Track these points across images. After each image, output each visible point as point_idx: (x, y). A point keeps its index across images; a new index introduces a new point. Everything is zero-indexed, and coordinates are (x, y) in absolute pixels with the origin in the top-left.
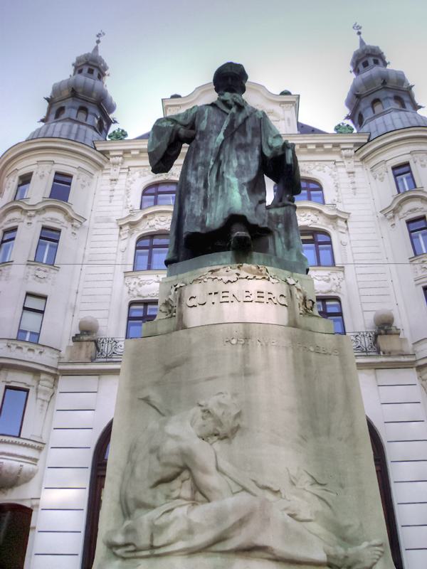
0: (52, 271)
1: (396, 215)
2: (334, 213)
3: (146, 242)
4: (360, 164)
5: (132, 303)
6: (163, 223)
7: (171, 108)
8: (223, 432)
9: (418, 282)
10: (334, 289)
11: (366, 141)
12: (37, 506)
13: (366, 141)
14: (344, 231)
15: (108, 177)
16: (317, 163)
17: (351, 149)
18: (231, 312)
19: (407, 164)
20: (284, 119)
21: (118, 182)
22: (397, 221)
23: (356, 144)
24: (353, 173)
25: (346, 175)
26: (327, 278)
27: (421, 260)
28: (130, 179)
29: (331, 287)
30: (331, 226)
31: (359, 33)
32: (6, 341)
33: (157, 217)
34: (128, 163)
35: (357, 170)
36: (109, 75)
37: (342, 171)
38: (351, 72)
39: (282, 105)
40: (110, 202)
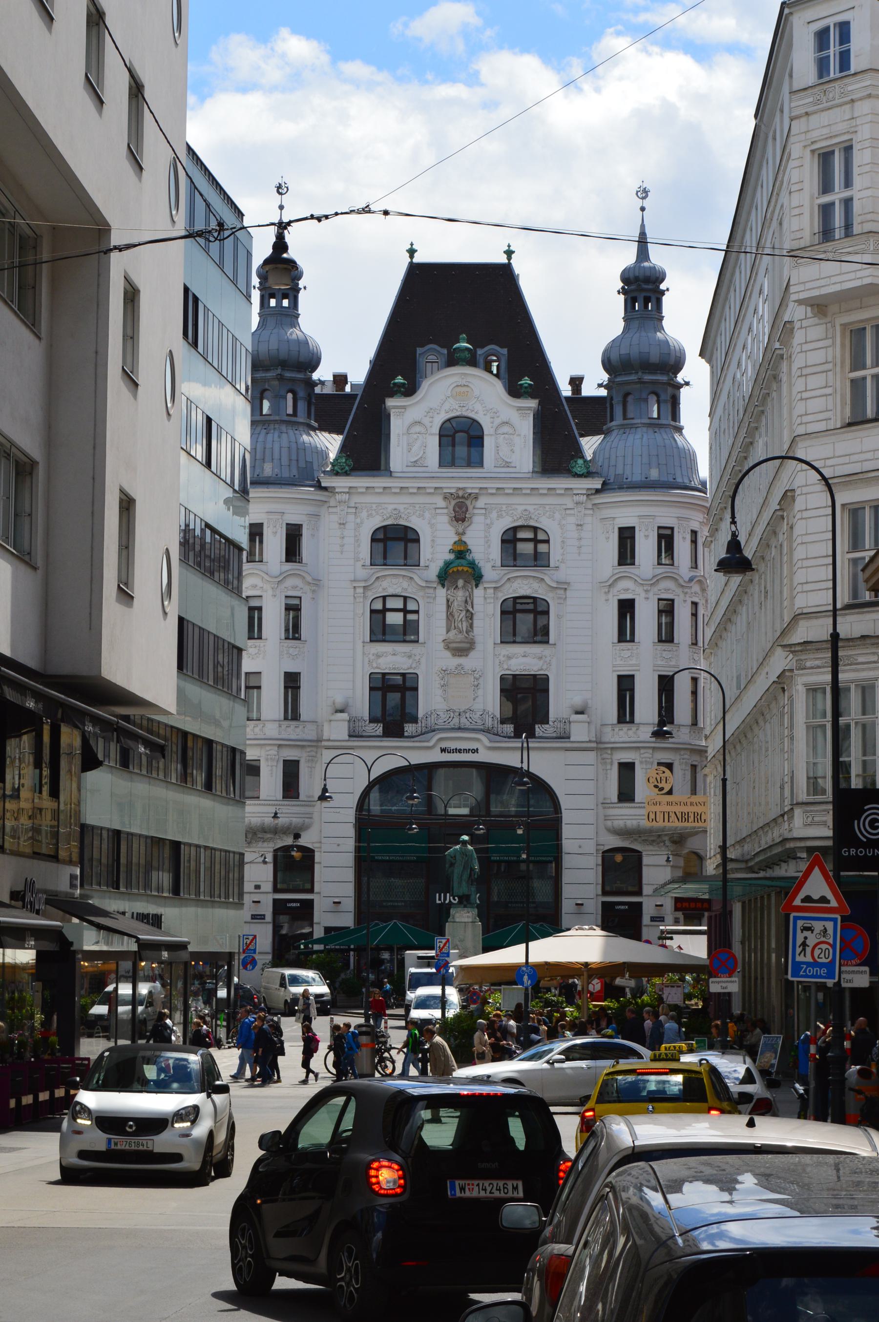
0: (301, 646)
1: (611, 589)
2: (554, 585)
3: (378, 606)
4: (591, 512)
5: (371, 674)
6: (395, 586)
7: (397, 410)
8: (461, 941)
9: (614, 669)
10: (544, 667)
11: (599, 486)
12: (321, 848)
13: (599, 486)
14: (562, 602)
15: (335, 518)
16: (547, 507)
17: (583, 494)
18: (463, 920)
19: (634, 528)
20: (519, 435)
21: (347, 526)
22: (610, 596)
23: (588, 489)
24: (581, 525)
25: (574, 527)
26: (540, 655)
27: (622, 648)
28: (358, 521)
29: (543, 665)
30: (551, 595)
31: (643, 209)
32: (278, 722)
33: (389, 579)
34: (356, 499)
35: (588, 519)
36: (305, 288)
37: (572, 520)
38: (619, 292)
39: (520, 412)
40: (342, 552)
